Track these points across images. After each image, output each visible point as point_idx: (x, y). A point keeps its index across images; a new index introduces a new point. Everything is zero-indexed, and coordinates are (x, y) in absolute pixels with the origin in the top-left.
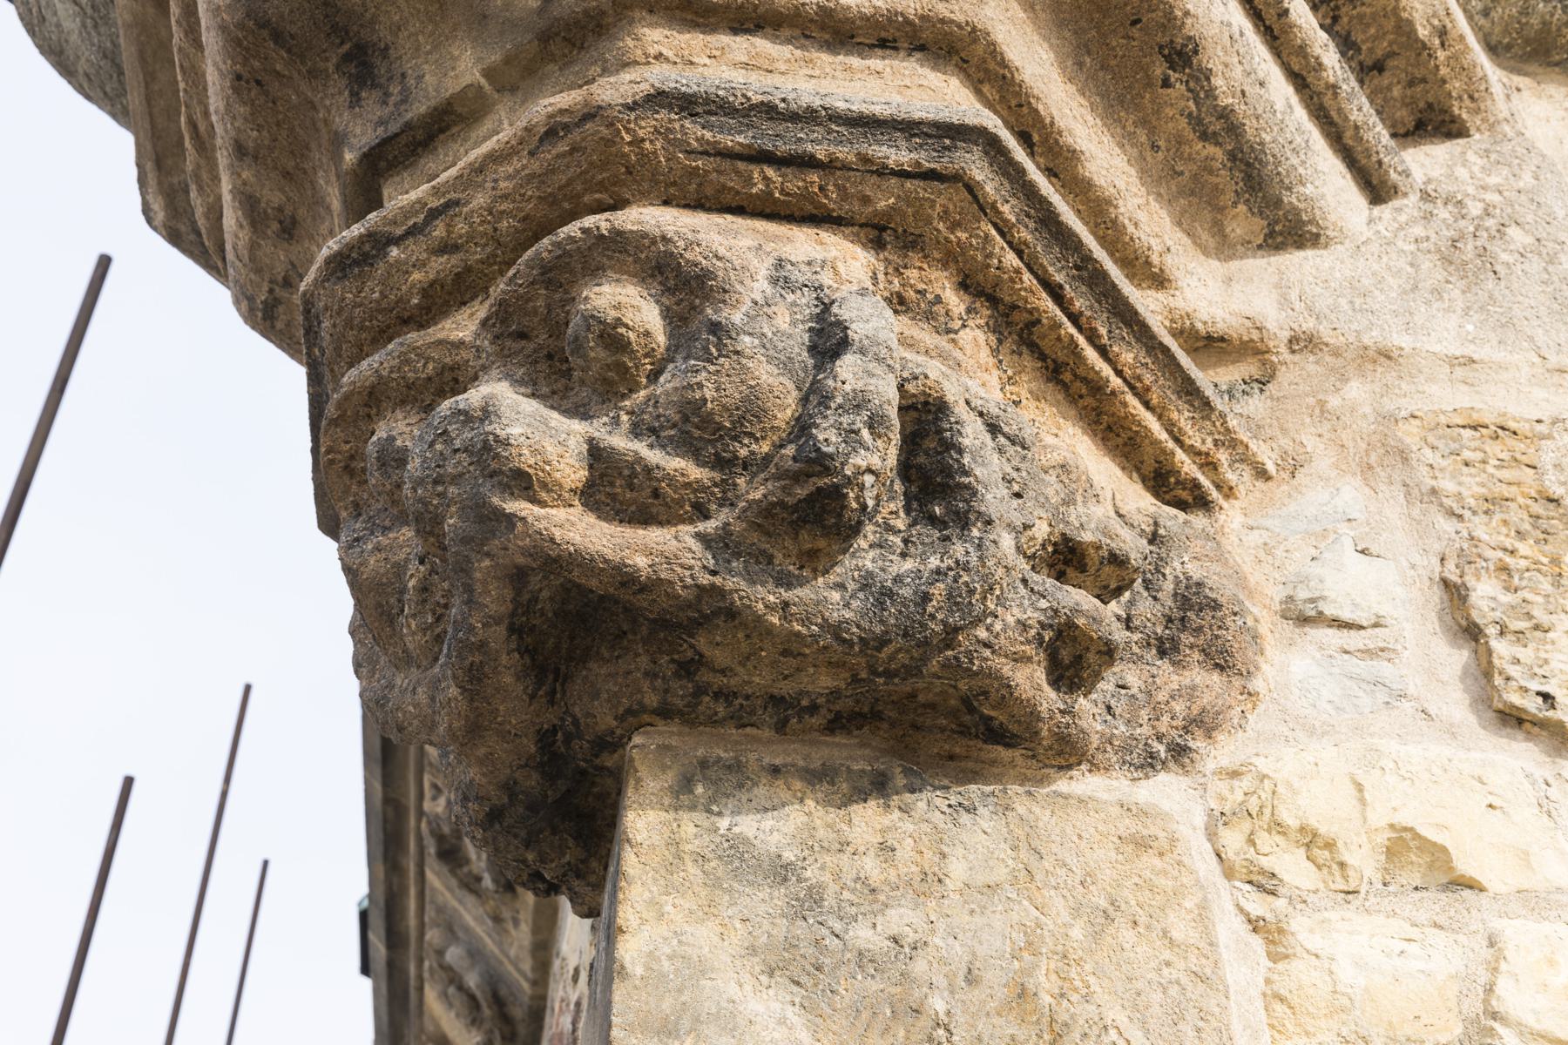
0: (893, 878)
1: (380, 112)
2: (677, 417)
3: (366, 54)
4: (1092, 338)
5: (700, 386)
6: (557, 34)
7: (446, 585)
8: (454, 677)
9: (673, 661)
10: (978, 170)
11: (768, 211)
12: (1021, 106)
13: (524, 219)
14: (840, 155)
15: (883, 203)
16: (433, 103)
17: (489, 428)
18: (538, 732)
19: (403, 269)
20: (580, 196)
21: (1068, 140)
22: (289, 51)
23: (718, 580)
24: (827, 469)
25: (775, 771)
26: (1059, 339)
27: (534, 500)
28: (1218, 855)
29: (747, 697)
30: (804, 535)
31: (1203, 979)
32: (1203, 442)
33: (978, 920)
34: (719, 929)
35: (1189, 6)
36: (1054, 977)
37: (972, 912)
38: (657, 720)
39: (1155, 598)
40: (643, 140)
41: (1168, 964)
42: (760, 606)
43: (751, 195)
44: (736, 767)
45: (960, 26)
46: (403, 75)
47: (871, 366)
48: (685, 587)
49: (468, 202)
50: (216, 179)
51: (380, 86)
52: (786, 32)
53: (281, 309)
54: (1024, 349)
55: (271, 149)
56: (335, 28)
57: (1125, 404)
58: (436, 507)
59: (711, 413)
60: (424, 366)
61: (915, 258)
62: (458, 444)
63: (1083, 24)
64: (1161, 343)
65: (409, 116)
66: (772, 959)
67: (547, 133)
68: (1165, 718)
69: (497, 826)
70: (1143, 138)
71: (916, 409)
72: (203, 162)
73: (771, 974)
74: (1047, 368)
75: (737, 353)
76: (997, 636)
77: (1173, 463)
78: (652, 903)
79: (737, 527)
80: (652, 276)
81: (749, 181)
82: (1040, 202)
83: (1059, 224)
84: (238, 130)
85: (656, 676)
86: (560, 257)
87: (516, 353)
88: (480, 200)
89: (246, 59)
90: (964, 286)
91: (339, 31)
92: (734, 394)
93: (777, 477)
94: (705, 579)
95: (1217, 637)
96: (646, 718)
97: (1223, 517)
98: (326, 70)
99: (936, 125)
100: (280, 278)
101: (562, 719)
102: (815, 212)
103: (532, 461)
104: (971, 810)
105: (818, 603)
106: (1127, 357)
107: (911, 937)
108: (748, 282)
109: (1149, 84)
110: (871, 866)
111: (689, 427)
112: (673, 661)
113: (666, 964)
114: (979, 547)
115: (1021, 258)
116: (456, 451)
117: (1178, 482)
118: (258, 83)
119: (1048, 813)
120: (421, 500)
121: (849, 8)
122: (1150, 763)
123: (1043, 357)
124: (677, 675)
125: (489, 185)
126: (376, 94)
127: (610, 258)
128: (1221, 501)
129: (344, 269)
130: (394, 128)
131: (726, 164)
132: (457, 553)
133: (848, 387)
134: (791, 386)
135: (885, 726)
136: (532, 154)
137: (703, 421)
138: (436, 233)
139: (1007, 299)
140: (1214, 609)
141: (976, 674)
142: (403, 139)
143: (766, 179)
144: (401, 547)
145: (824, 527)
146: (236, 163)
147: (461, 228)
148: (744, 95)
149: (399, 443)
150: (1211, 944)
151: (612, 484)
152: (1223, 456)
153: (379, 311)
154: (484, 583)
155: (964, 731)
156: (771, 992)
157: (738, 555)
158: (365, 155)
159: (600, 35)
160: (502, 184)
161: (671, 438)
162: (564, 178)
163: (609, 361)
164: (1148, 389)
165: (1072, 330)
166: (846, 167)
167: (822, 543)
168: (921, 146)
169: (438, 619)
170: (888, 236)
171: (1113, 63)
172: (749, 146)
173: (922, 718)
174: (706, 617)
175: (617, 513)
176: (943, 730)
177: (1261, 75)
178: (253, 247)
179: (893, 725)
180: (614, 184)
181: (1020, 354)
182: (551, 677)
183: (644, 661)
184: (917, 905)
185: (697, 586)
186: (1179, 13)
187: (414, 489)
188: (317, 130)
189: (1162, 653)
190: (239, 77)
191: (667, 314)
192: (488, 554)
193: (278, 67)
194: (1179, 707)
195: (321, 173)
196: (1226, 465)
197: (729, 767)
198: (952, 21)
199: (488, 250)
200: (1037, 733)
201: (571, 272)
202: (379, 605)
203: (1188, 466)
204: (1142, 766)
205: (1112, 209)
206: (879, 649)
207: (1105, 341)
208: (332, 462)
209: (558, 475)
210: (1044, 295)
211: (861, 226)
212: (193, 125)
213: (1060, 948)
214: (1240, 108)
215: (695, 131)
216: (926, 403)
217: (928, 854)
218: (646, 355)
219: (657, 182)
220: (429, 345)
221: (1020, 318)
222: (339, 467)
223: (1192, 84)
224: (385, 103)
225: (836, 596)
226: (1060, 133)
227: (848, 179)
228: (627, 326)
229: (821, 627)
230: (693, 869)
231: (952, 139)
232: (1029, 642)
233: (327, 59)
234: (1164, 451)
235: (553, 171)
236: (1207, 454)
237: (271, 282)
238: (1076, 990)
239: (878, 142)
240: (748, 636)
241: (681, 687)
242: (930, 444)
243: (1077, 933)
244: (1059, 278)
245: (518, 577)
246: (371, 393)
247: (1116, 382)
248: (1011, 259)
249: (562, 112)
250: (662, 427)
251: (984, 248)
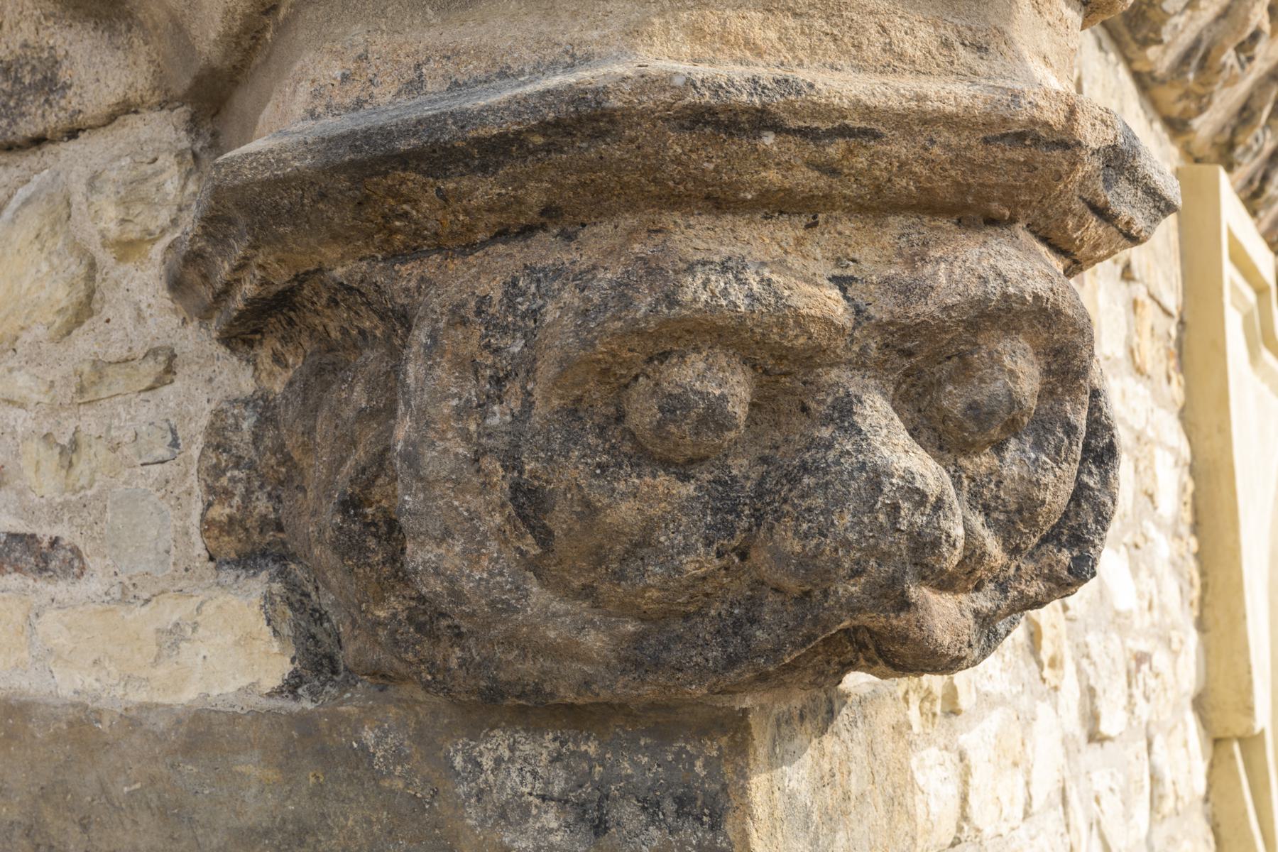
2: (1013, 507)
13: (926, 189)
17: (944, 524)
19: (764, 159)
20: (989, 200)
49: (888, 144)
60: (797, 336)
87: (894, 370)
88: (900, 148)
93: (1048, 578)
127: (1032, 326)
129: (698, 122)
138: (830, 150)
147: (861, 162)
160: (936, 150)
202: (601, 547)
220: (813, 319)
249: (1046, 124)
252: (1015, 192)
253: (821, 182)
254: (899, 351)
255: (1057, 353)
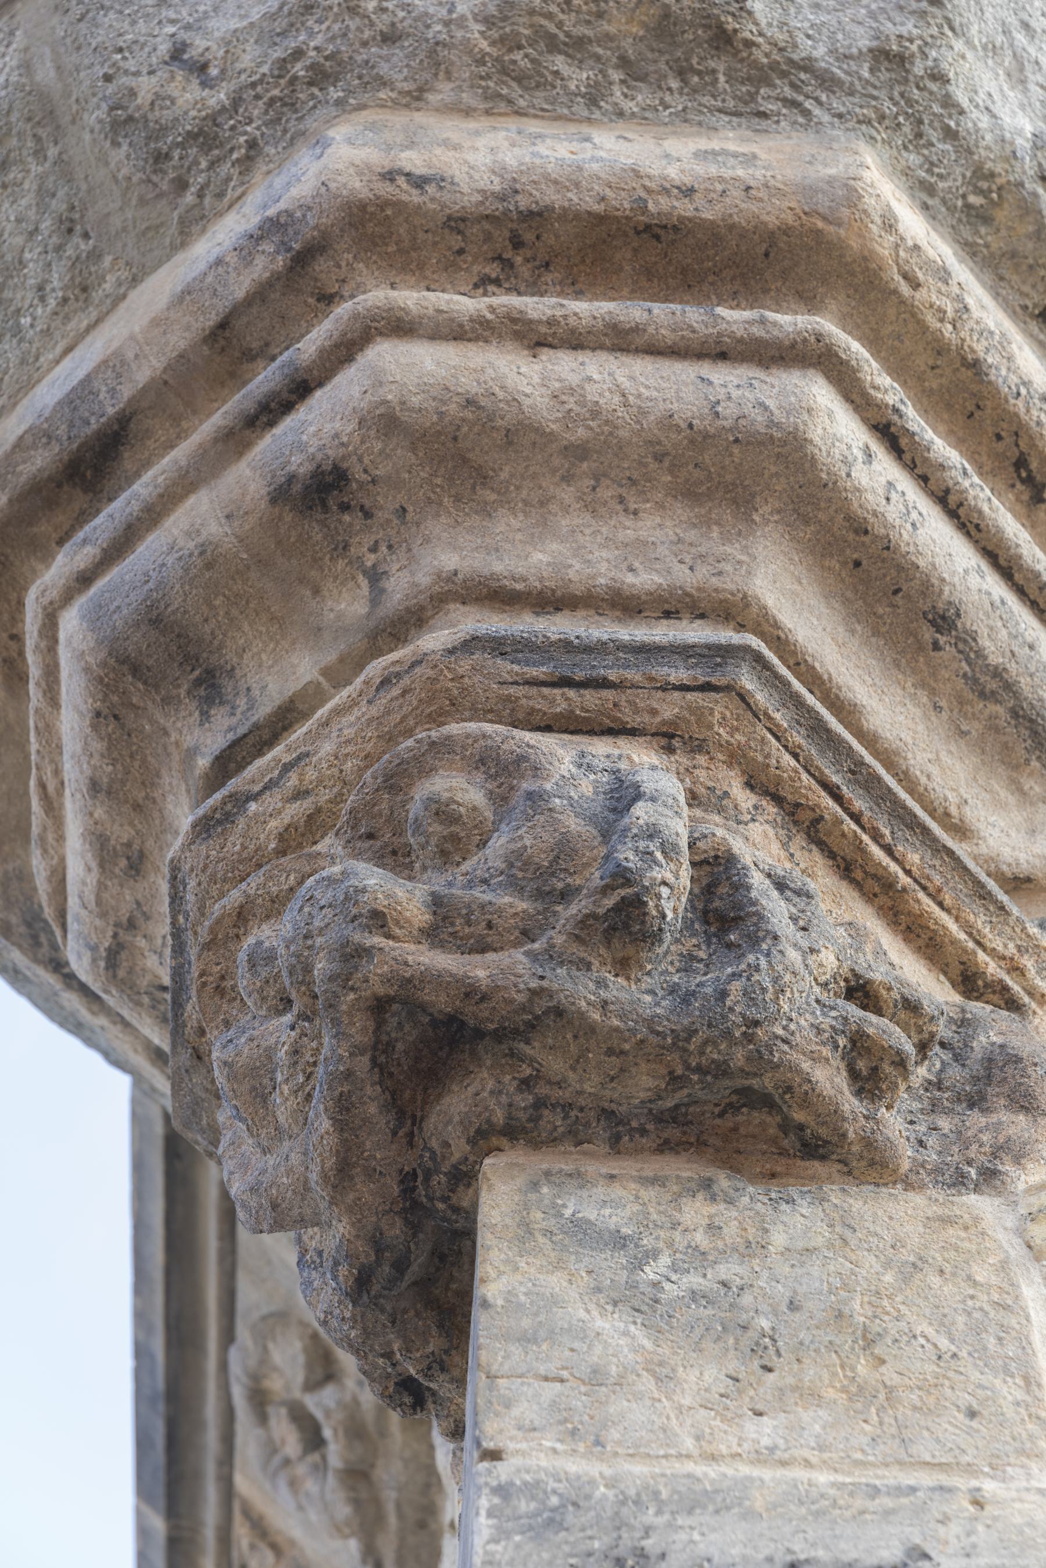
0: (720, 1244)
1: (227, 722)
2: (504, 866)
3: (214, 677)
4: (876, 837)
5: (521, 838)
6: (384, 631)
7: (314, 1044)
8: (326, 1110)
9: (514, 1078)
10: (748, 682)
11: (572, 728)
12: (798, 664)
13: (366, 757)
14: (629, 676)
15: (668, 713)
16: (277, 703)
18: (401, 1171)
21: (846, 694)
22: (145, 683)
23: (545, 983)
24: (628, 880)
25: (612, 1177)
26: (843, 835)
27: (388, 936)
28: (1029, 1247)
29: (581, 1109)
30: (616, 943)
31: (1006, 1308)
32: (1005, 946)
33: (799, 1271)
34: (568, 1277)
35: (945, 575)
36: (866, 1307)
37: (793, 1266)
38: (504, 1142)
39: (963, 1065)
40: (462, 677)
41: (972, 1297)
42: (583, 1003)
43: (556, 714)
44: (576, 1174)
45: (733, 594)
46: (248, 689)
47: (660, 809)
48: (519, 991)
49: (316, 752)
50: (61, 838)
51: (228, 702)
52: (581, 613)
53: (124, 955)
54: (814, 847)
55: (123, 783)
56: (187, 658)
57: (918, 901)
58: (307, 958)
59: (530, 857)
61: (702, 759)
62: (322, 903)
63: (849, 594)
64: (944, 846)
65: (255, 719)
66: (615, 1295)
67: (382, 683)
68: (974, 1147)
69: (365, 1298)
70: (925, 699)
71: (709, 863)
72: (49, 823)
73: (615, 1304)
74: (838, 867)
75: (550, 810)
76: (793, 1034)
77: (977, 964)
78: (507, 1262)
79: (559, 940)
80: (477, 768)
81: (553, 702)
82: (808, 712)
83: (828, 731)
84: (95, 768)
85: (500, 1092)
86: (399, 764)
88: (327, 748)
89: (106, 695)
90: (749, 785)
91: (190, 660)
92: (549, 838)
94: (534, 984)
95: (1020, 1084)
96: (495, 1141)
97: (1037, 1021)
98: (179, 696)
99: (709, 647)
100: (124, 920)
101: (421, 1156)
102: (612, 725)
103: (386, 903)
104: (791, 1201)
105: (632, 1002)
106: (914, 858)
107: (738, 1281)
108: (556, 763)
109: (920, 648)
110: (700, 1238)
111: (514, 871)
112: (514, 1078)
113: (523, 1298)
114: (768, 955)
115: (798, 761)
116: (322, 908)
117: (986, 985)
118: (116, 717)
119: (861, 1203)
120: (293, 955)
121: (634, 585)
122: (960, 1181)
123: (831, 855)
124: (519, 1089)
125: (334, 734)
126: (225, 710)
128: (1034, 1005)
130: (241, 731)
131: (534, 691)
132: (326, 991)
133: (641, 822)
134: (595, 832)
135: (711, 1150)
136: (369, 702)
137: (525, 864)
139: (789, 797)
140: (1016, 1062)
141: (778, 1066)
142: (250, 740)
143: (567, 699)
144: (272, 1034)
145: (630, 933)
146: (90, 802)
147: (311, 775)
148: (544, 636)
149: (267, 944)
150: (1012, 1285)
151: (452, 924)
152: (1028, 963)
153: (240, 862)
154: (349, 1014)
155: (783, 1153)
156: (616, 1316)
157: (561, 964)
158: (217, 758)
159: (420, 627)
160: (346, 732)
161: (500, 883)
162: (398, 717)
163: (445, 833)
164: (939, 890)
165: (854, 826)
166: (633, 686)
167: (630, 950)
168: (696, 665)
169: (308, 1078)
170: (676, 743)
171: (884, 629)
172: (552, 674)
173: (735, 1115)
174: (537, 1018)
175: (459, 947)
176: (764, 1153)
177: (1029, 639)
178: (101, 886)
179: (717, 1151)
180: (440, 716)
181: (810, 851)
182: (409, 1122)
183: (490, 1084)
184: (743, 1262)
185: (529, 989)
186: (936, 582)
187: (287, 947)
188: (169, 755)
189: (971, 1106)
190: (98, 714)
191: (490, 795)
192: (352, 989)
193: (134, 700)
194: (985, 1138)
195: (170, 798)
196: (1033, 972)
197: (570, 1175)
198: (724, 590)
199: (335, 790)
200: (844, 1136)
201: (410, 776)
202: (254, 1089)
203: (992, 969)
204: (954, 1185)
205: (901, 761)
206: (688, 1040)
207: (888, 839)
208: (204, 984)
209: (408, 914)
210: (823, 794)
211: (653, 735)
212: (42, 786)
213: (873, 1288)
214: (1012, 667)
215: (506, 668)
216: (716, 857)
217: (752, 1231)
218: (476, 827)
219: (476, 710)
221: (806, 816)
222: (209, 988)
223: (961, 646)
224: (233, 714)
225: (648, 998)
226: (839, 688)
227: (637, 696)
228: (459, 804)
229: (636, 1022)
230: (541, 1240)
231: (722, 657)
232: (824, 1044)
233: (179, 686)
234: (965, 951)
235: (388, 713)
236: (1012, 959)
237: (116, 925)
238: (888, 1313)
239: (659, 664)
240: (575, 1037)
241: (523, 1100)
242: (723, 890)
243: (888, 1278)
244: (836, 779)
245: (379, 1007)
246: (239, 913)
247: (904, 880)
248: (787, 759)
250: (492, 876)
251: (762, 750)
252: (418, 712)
253: (306, 805)
254: (360, 837)
255: (482, 761)
